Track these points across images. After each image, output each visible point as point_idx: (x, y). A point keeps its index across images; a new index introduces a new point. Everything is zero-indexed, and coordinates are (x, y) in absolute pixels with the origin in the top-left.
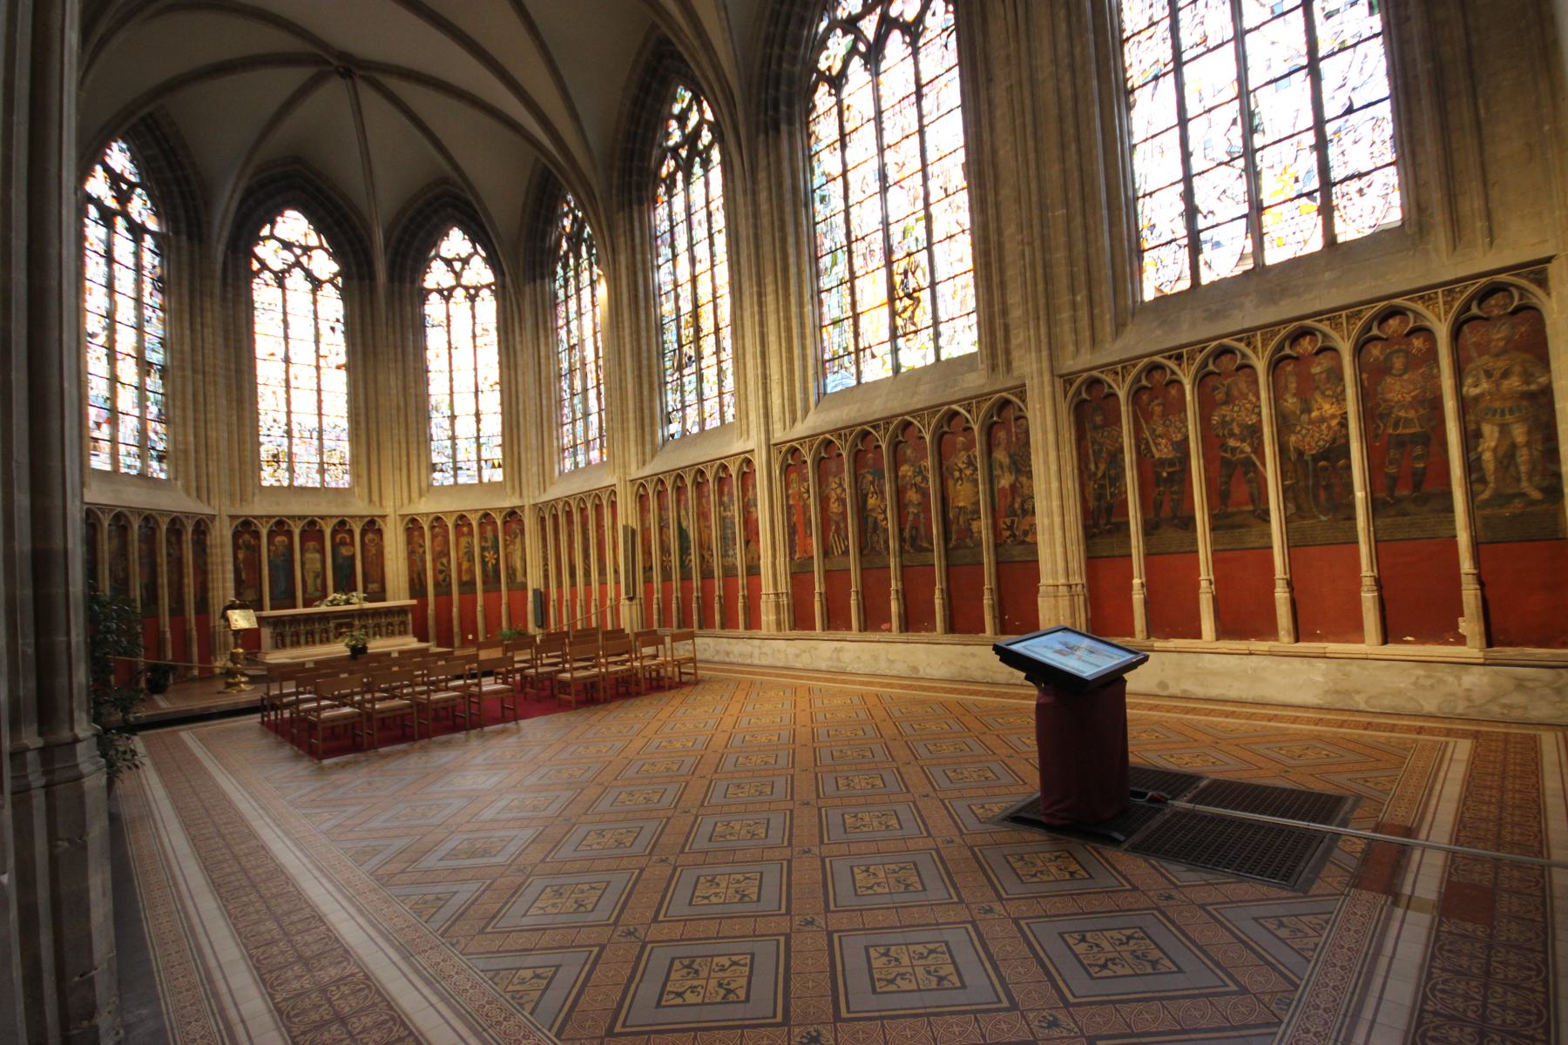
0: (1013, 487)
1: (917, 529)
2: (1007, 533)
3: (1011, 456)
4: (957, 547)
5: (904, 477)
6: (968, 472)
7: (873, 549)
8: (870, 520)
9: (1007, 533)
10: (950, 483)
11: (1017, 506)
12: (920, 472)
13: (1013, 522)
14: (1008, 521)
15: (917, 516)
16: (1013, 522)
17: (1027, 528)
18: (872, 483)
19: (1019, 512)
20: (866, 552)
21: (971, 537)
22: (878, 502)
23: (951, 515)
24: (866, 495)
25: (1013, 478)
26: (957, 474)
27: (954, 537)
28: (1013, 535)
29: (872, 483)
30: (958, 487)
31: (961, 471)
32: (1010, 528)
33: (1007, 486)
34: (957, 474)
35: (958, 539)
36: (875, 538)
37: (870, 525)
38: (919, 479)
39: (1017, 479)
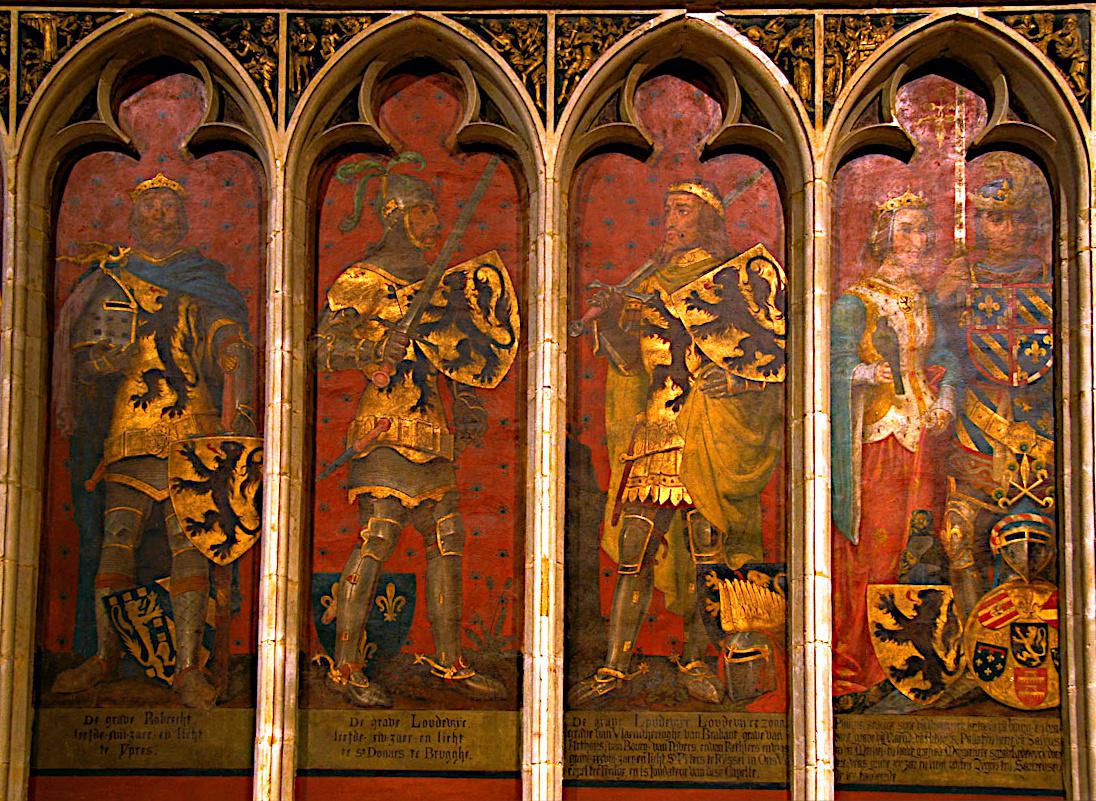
0: (940, 444)
1: (410, 587)
2: (898, 654)
3: (943, 315)
4: (619, 698)
5: (356, 321)
6: (718, 349)
7: (125, 665)
8: (118, 516)
9: (898, 654)
10: (621, 386)
11: (952, 532)
12: (454, 314)
13: (930, 601)
14: (908, 599)
15: (411, 525)
16: (930, 601)
17: (999, 638)
18: (160, 326)
19: (964, 562)
20: (68, 682)
21: (711, 659)
22: (184, 427)
23: (610, 544)
24: (112, 384)
25: (945, 405)
26: (658, 349)
27: (619, 645)
28: (927, 665)
29: (160, 326)
30: (661, 412)
31: (678, 336)
32: (918, 629)
33: (911, 440)
34: (658, 349)
35: (637, 656)
36: (142, 615)
37: (118, 544)
38: (445, 343)
39: (961, 414)
